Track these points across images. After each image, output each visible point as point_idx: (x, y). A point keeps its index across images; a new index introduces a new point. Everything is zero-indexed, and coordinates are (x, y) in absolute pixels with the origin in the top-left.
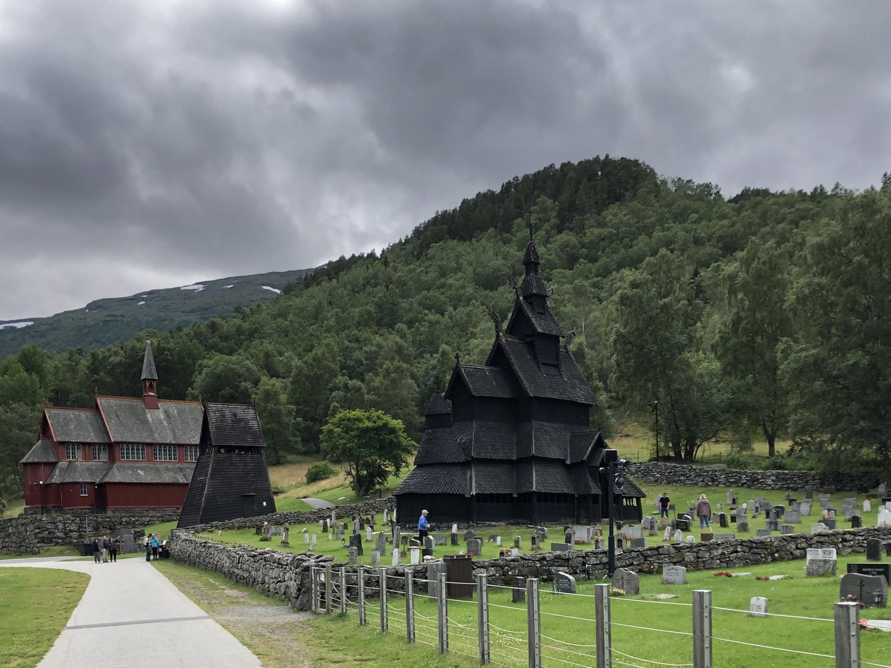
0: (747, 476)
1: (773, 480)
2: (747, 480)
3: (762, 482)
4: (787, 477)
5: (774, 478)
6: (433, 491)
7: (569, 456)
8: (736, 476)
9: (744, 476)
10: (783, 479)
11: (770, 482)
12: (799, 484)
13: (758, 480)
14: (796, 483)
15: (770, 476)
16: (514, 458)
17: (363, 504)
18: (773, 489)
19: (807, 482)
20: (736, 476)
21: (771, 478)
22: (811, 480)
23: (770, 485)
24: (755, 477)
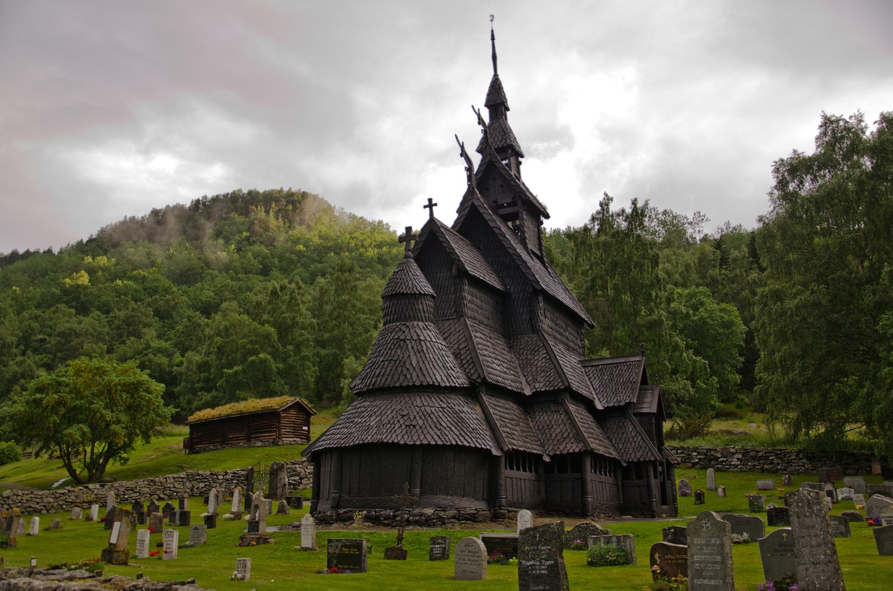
0: (698, 453)
1: (738, 459)
2: (699, 459)
3: (723, 461)
4: (760, 454)
5: (740, 456)
6: (432, 438)
7: (595, 396)
8: (682, 453)
9: (695, 454)
10: (753, 458)
11: (735, 462)
12: (778, 464)
13: (717, 458)
14: (772, 463)
15: (734, 454)
16: (528, 392)
17: (146, 482)
18: (741, 471)
19: (789, 462)
20: (682, 453)
21: (736, 456)
22: (795, 459)
23: (736, 466)
24: (712, 455)
